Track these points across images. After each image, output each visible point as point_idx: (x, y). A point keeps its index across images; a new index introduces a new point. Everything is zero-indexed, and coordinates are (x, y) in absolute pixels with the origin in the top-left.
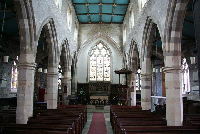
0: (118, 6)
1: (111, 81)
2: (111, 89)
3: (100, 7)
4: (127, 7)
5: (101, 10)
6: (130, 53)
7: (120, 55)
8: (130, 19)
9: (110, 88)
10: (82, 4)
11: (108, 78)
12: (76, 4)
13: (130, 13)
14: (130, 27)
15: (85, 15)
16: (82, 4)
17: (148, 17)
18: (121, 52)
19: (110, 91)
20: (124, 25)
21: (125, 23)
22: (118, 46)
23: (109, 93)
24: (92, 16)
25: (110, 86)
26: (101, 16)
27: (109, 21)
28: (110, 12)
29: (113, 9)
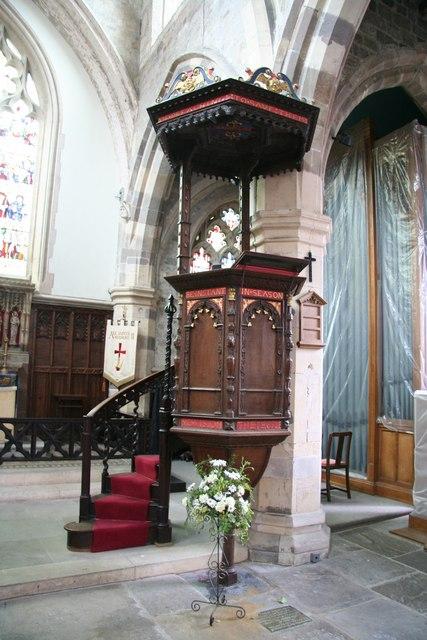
1: (36, 281)
2: (36, 334)
6: (142, 169)
7: (113, 113)
9: (25, 323)
11: (15, 254)
18: (122, 96)
19: (23, 348)
22: (112, 55)
23: (20, 360)
25: (27, 309)
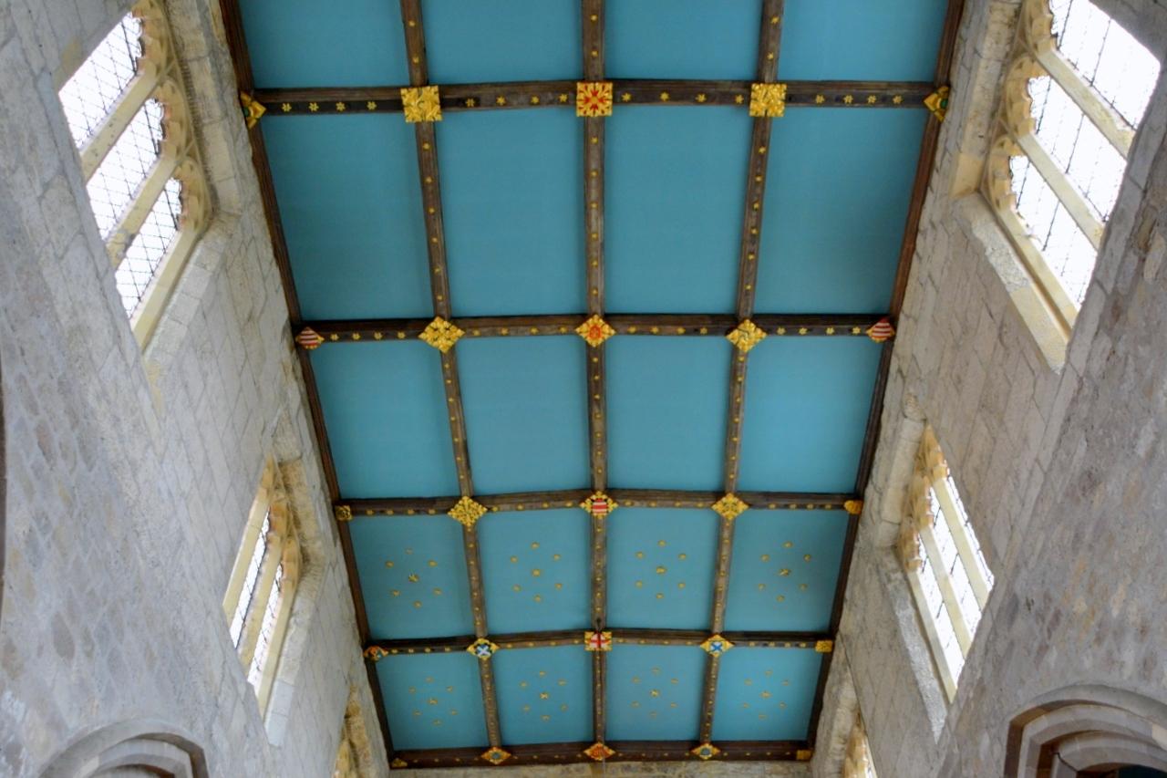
0: (773, 516)
3: (596, 539)
4: (854, 523)
5: (597, 584)
8: (904, 614)
10: (421, 504)
12: (360, 505)
13: (891, 563)
14: (928, 683)
15: (448, 657)
16: (421, 504)
17: (1016, 732)
20: (836, 745)
21: (838, 720)
24: (512, 661)
26: (598, 662)
27: (681, 725)
28: (692, 617)
29: (717, 567)
